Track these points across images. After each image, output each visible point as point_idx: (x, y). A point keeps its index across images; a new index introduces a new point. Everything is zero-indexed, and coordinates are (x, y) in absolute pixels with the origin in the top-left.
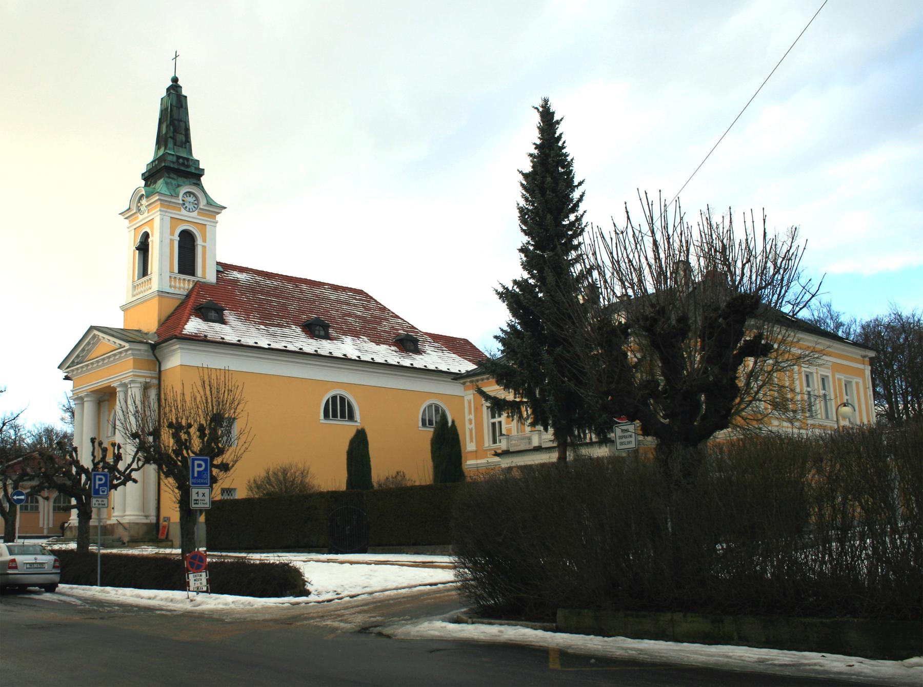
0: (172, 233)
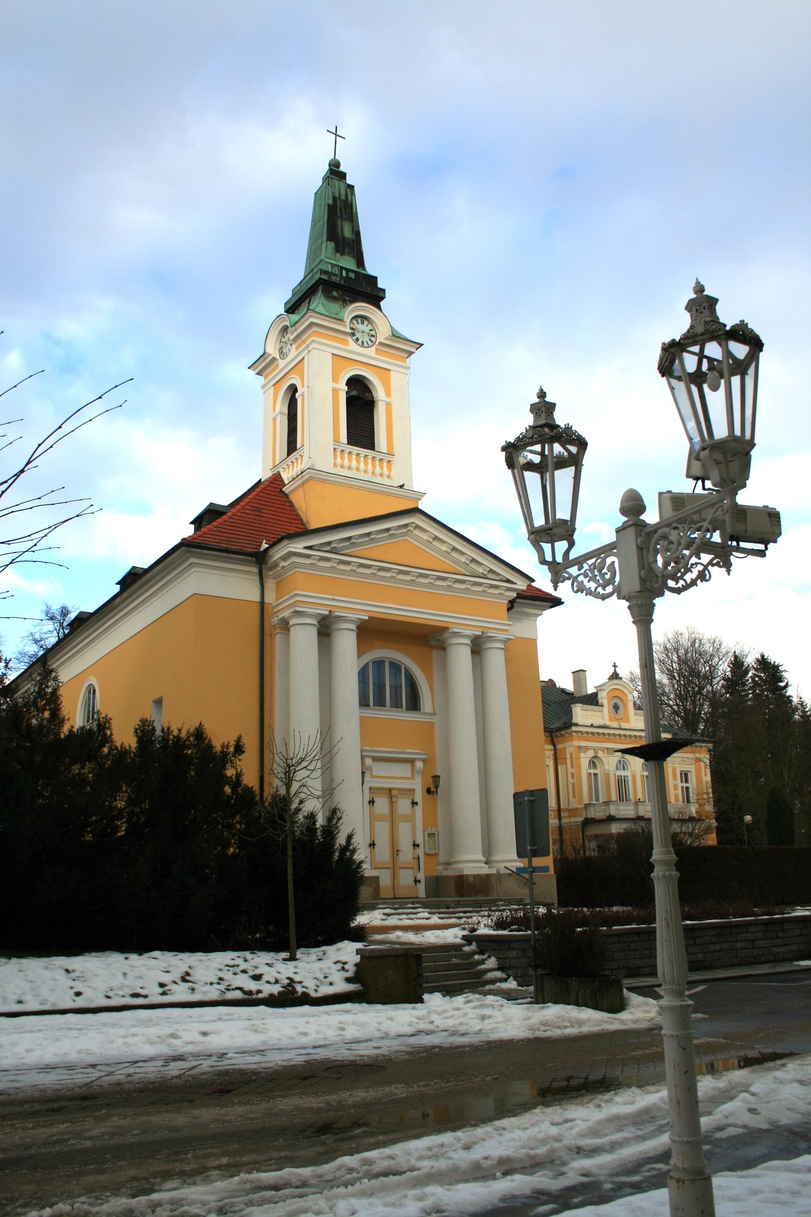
0: (335, 379)
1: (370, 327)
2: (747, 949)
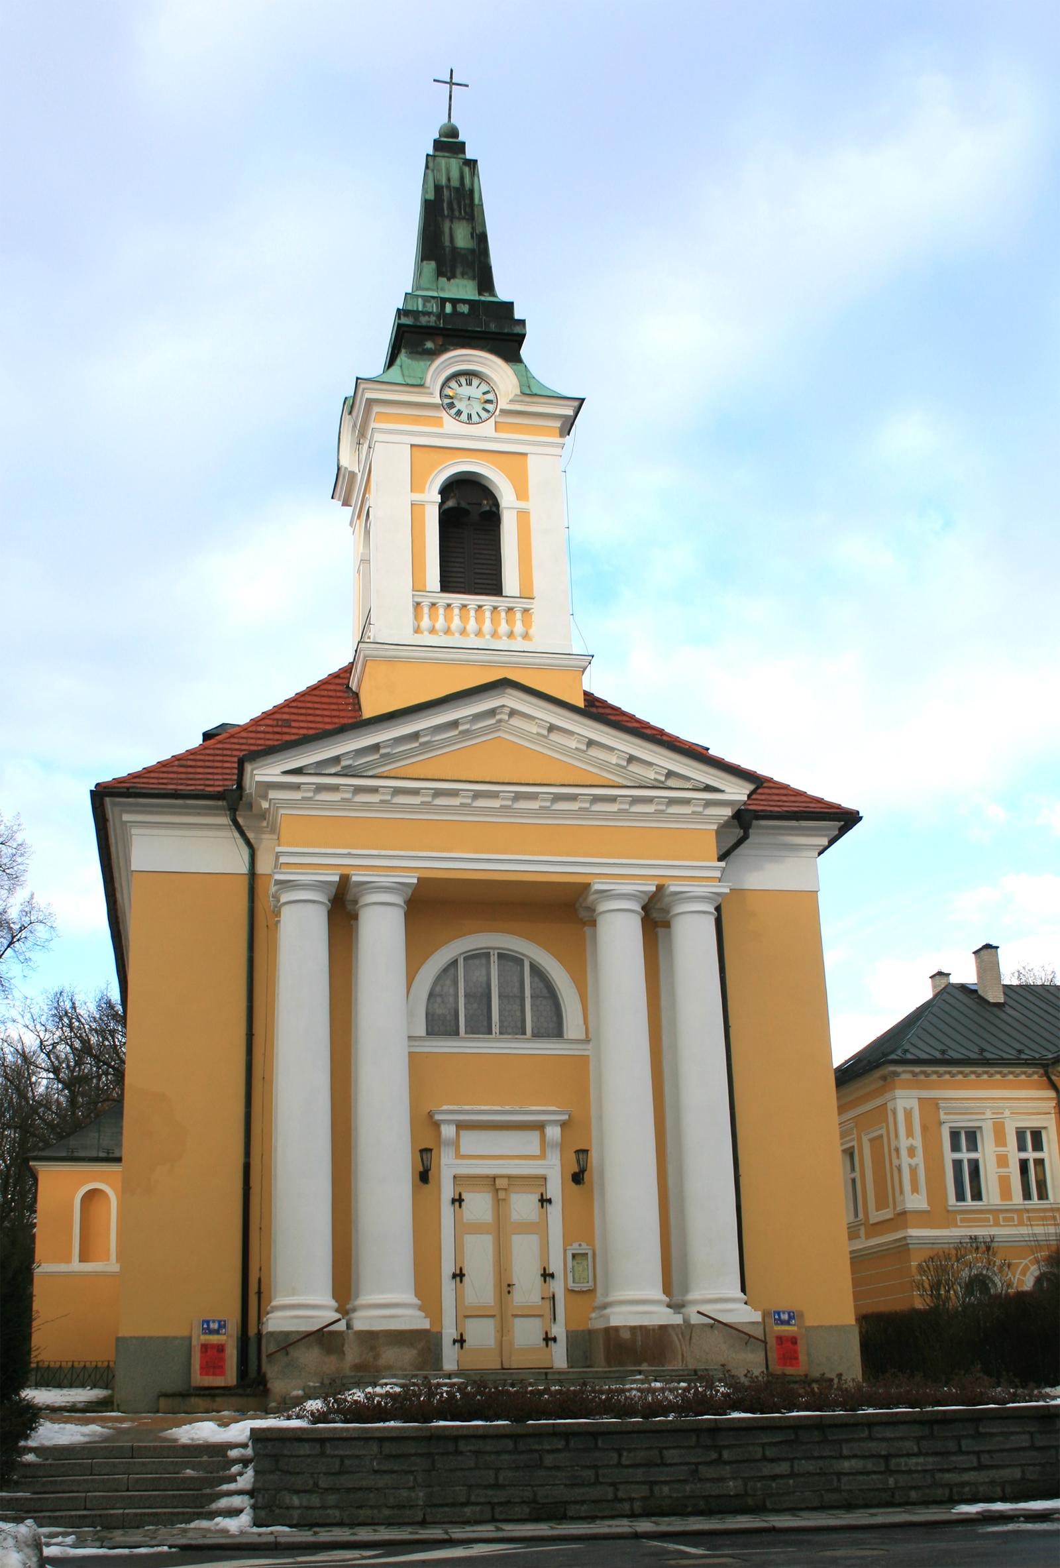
0: (416, 485)
1: (484, 388)
2: (869, 1473)
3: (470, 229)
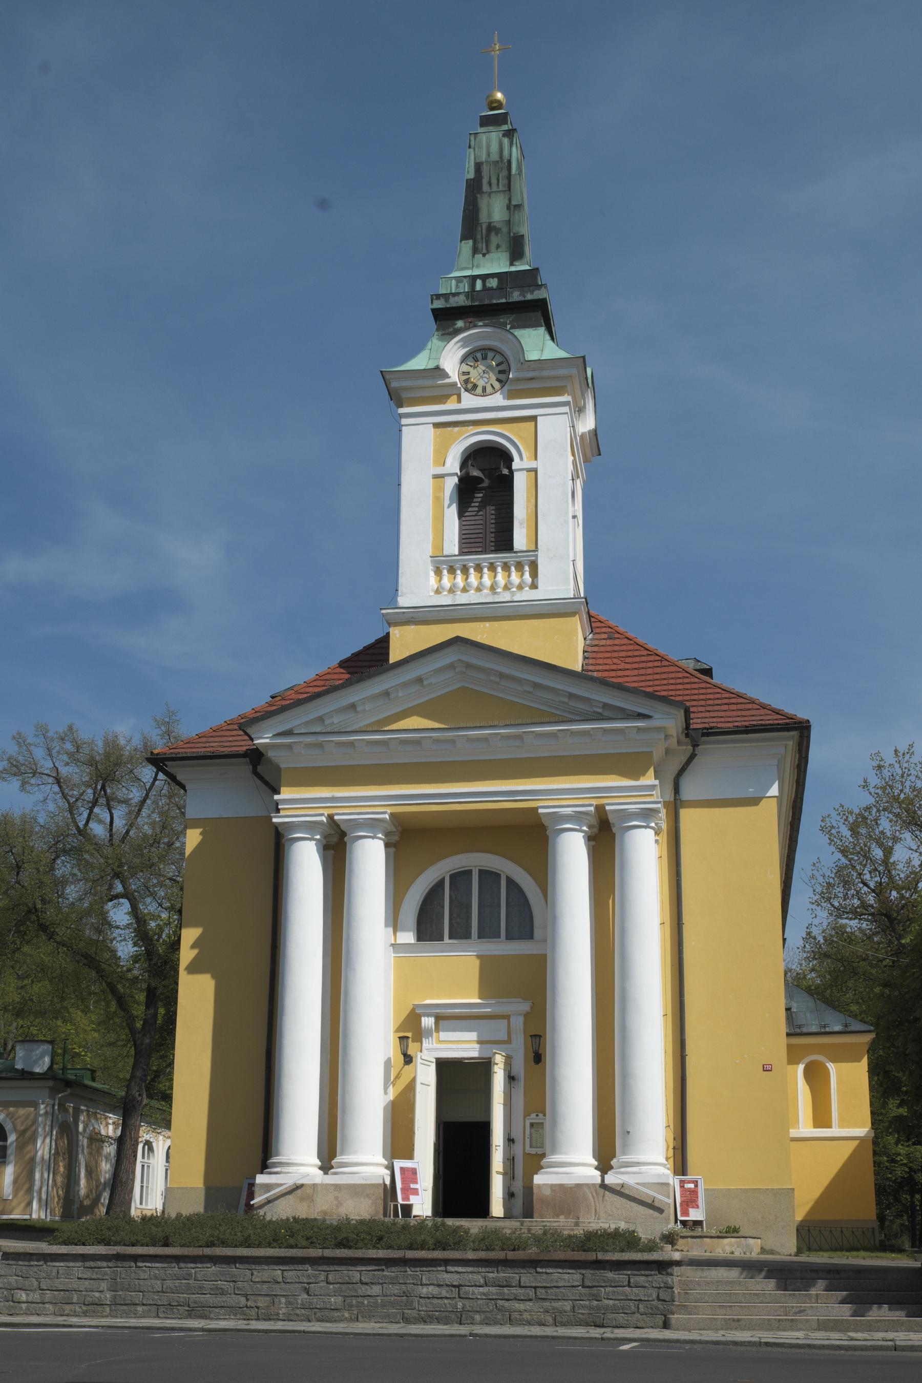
3: (507, 202)
